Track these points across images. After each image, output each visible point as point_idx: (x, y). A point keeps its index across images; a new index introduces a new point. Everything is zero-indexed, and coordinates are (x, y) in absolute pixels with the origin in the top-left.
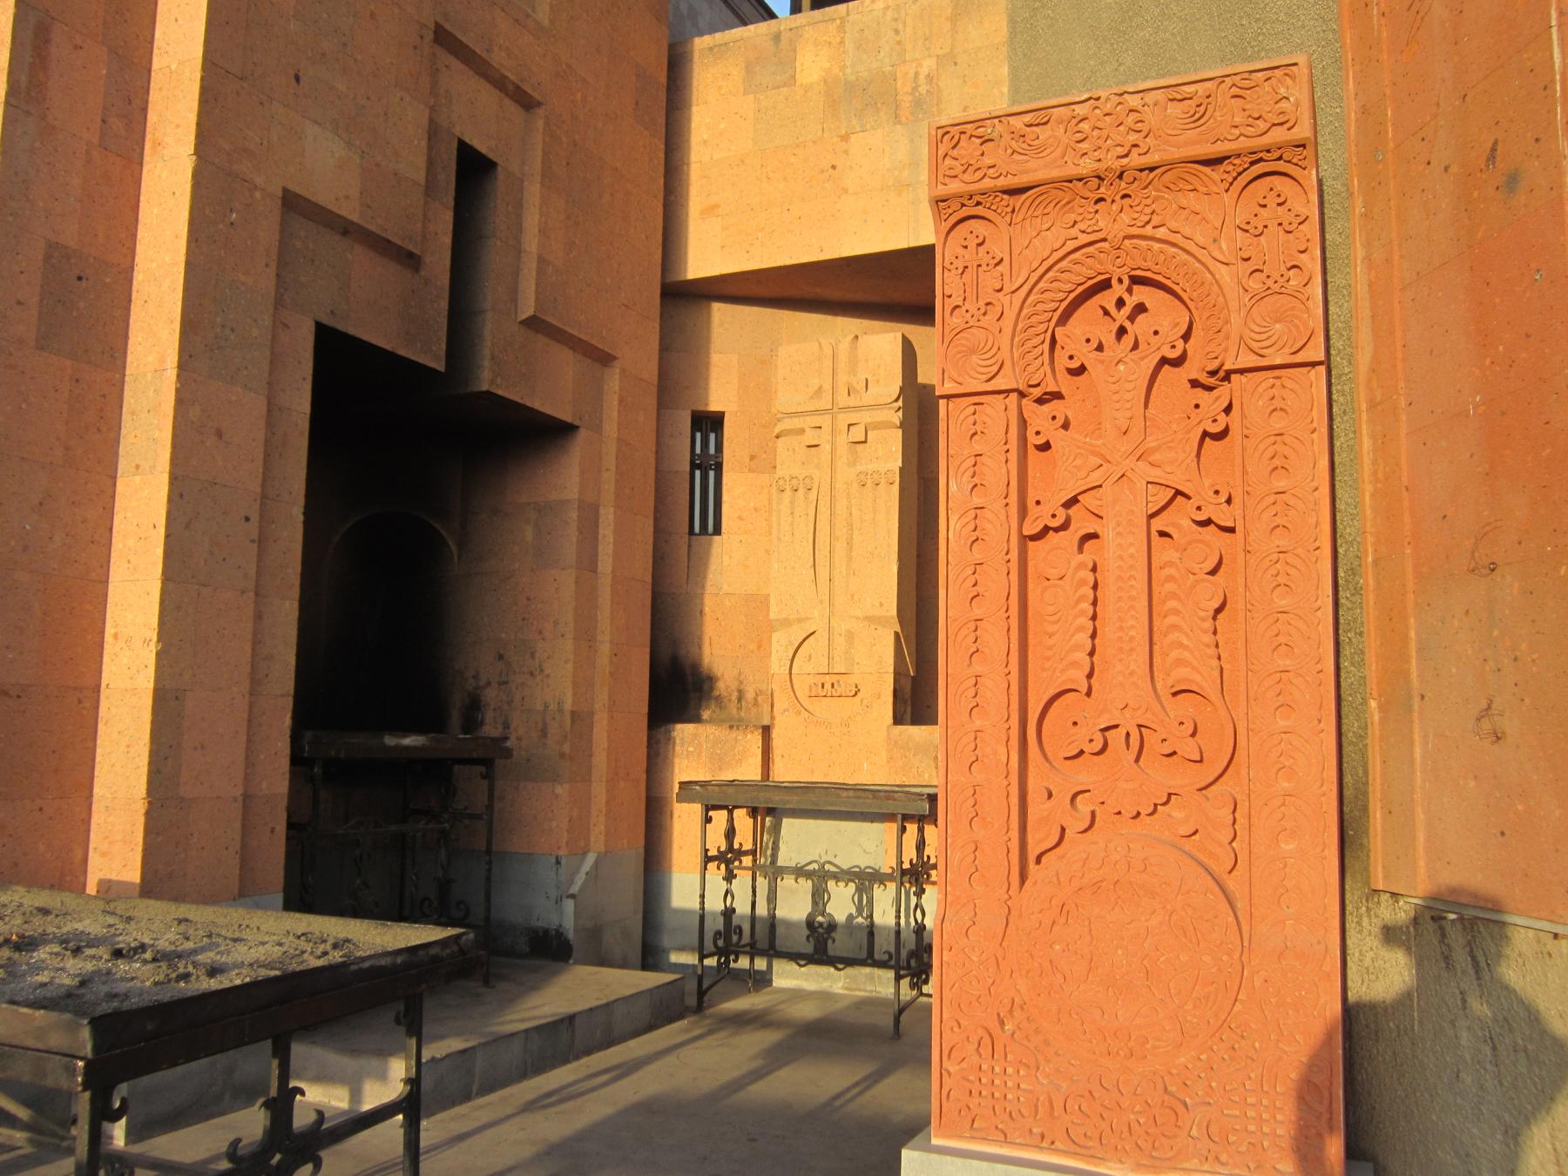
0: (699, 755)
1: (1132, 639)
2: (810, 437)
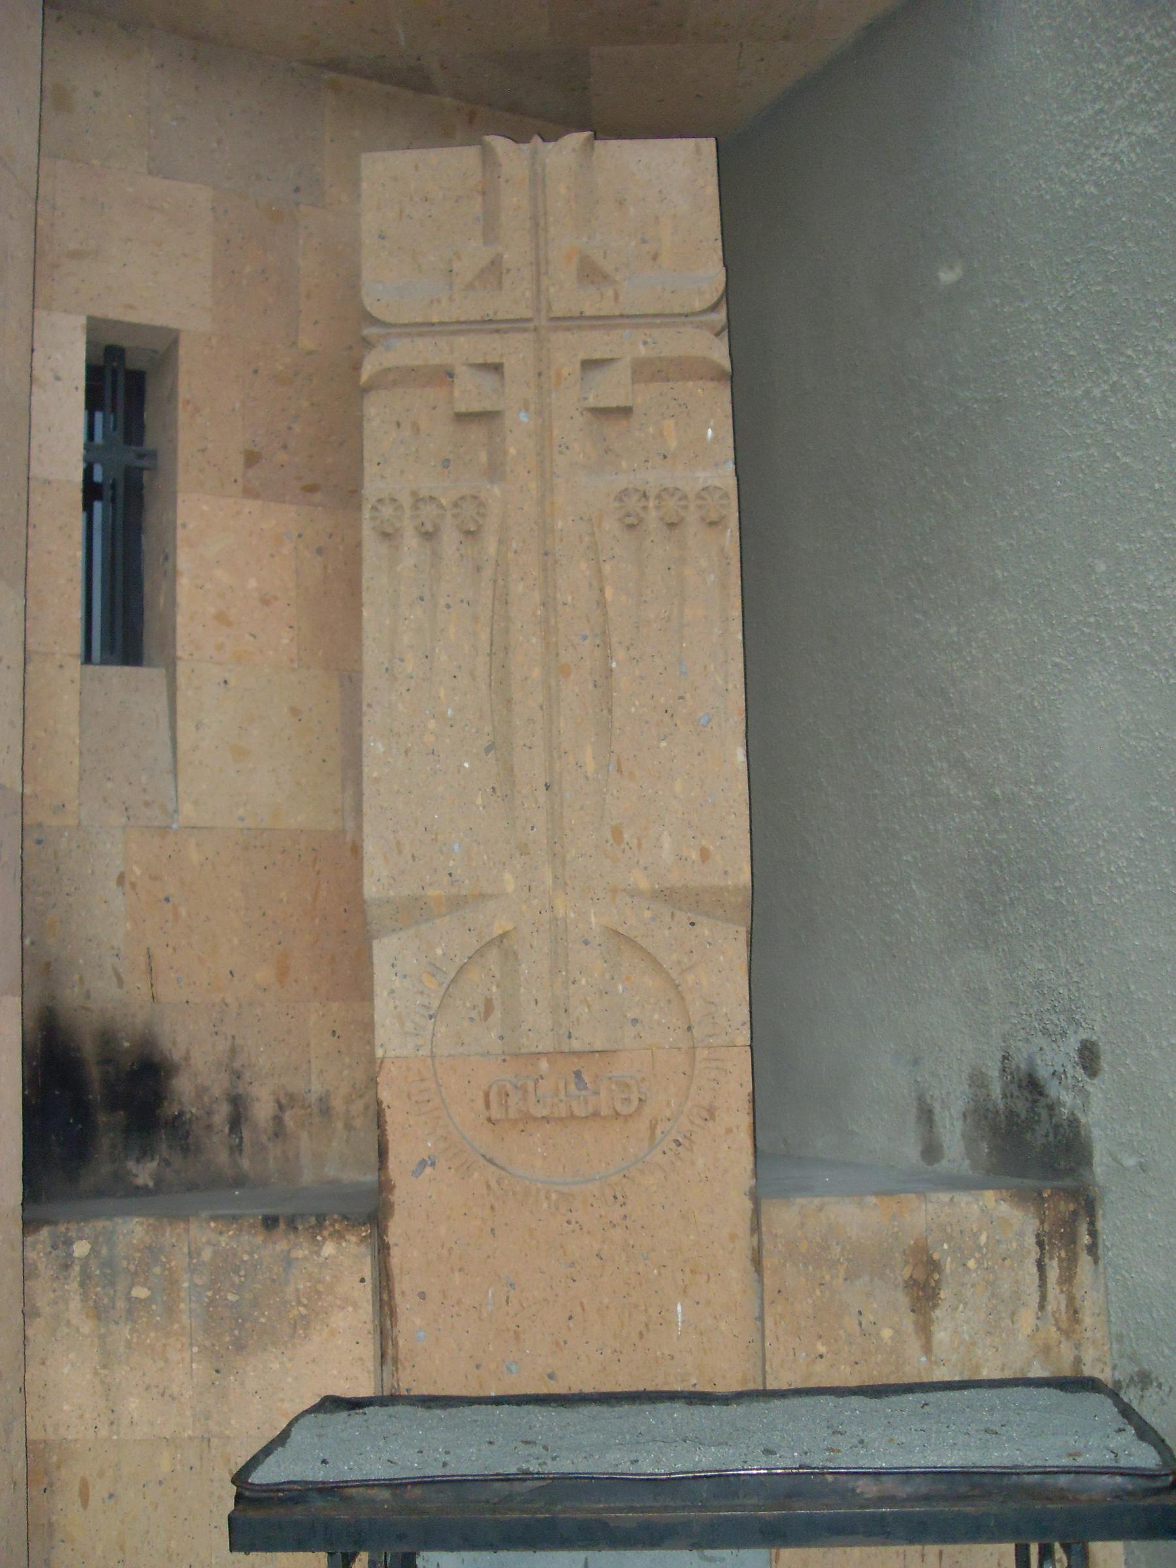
0: (170, 1311)
2: (471, 392)
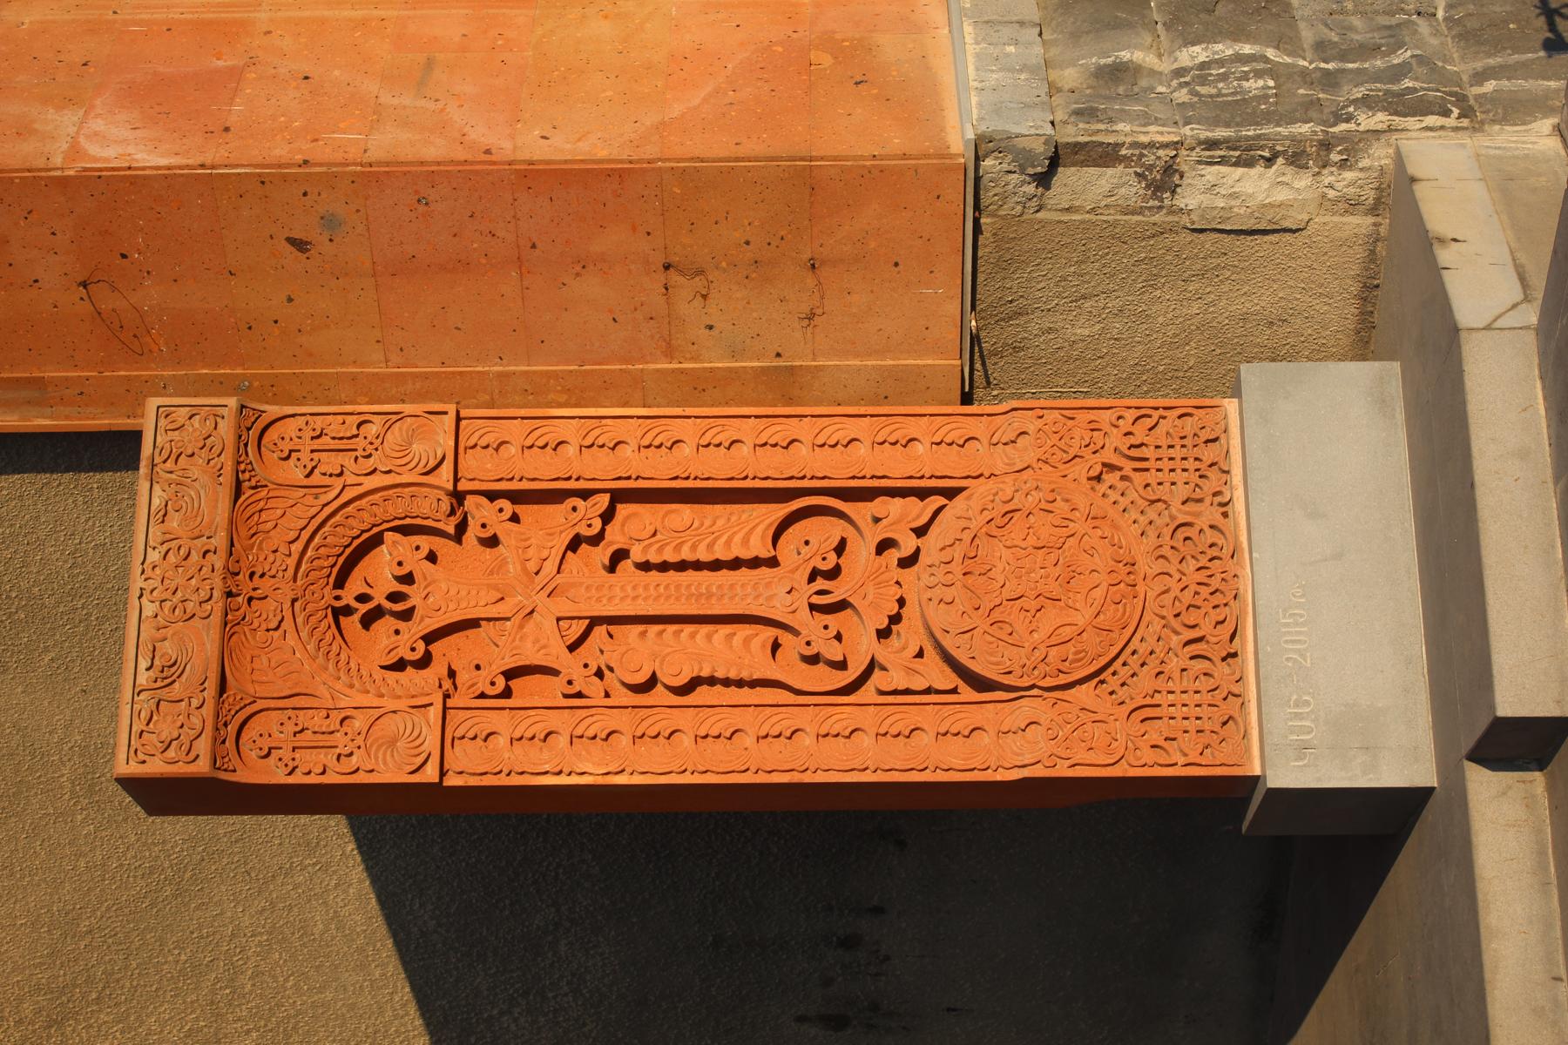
1: (720, 587)
